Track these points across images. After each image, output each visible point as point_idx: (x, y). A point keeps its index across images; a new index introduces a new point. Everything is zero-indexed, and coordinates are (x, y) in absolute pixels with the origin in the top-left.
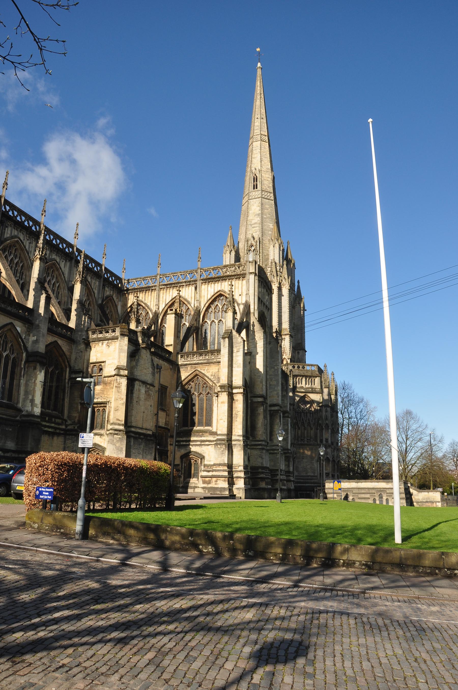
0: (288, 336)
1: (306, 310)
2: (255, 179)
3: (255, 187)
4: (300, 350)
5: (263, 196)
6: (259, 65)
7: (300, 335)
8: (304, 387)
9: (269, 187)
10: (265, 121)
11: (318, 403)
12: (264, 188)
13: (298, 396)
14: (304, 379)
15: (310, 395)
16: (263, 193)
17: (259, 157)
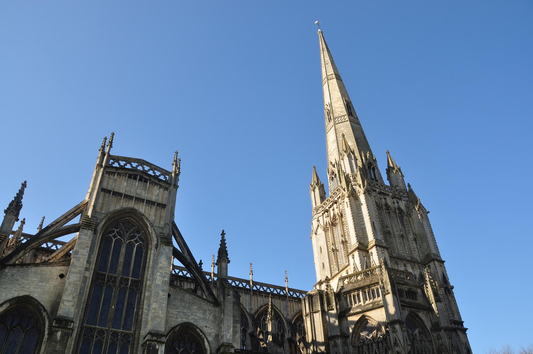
0: (374, 248)
1: (429, 212)
2: (328, 114)
3: (330, 120)
4: (430, 262)
5: (337, 122)
6: (319, 30)
7: (425, 244)
8: (363, 304)
9: (342, 112)
10: (330, 64)
11: (384, 323)
12: (336, 115)
13: (352, 322)
14: (361, 293)
15: (368, 314)
16: (337, 119)
17: (332, 96)
